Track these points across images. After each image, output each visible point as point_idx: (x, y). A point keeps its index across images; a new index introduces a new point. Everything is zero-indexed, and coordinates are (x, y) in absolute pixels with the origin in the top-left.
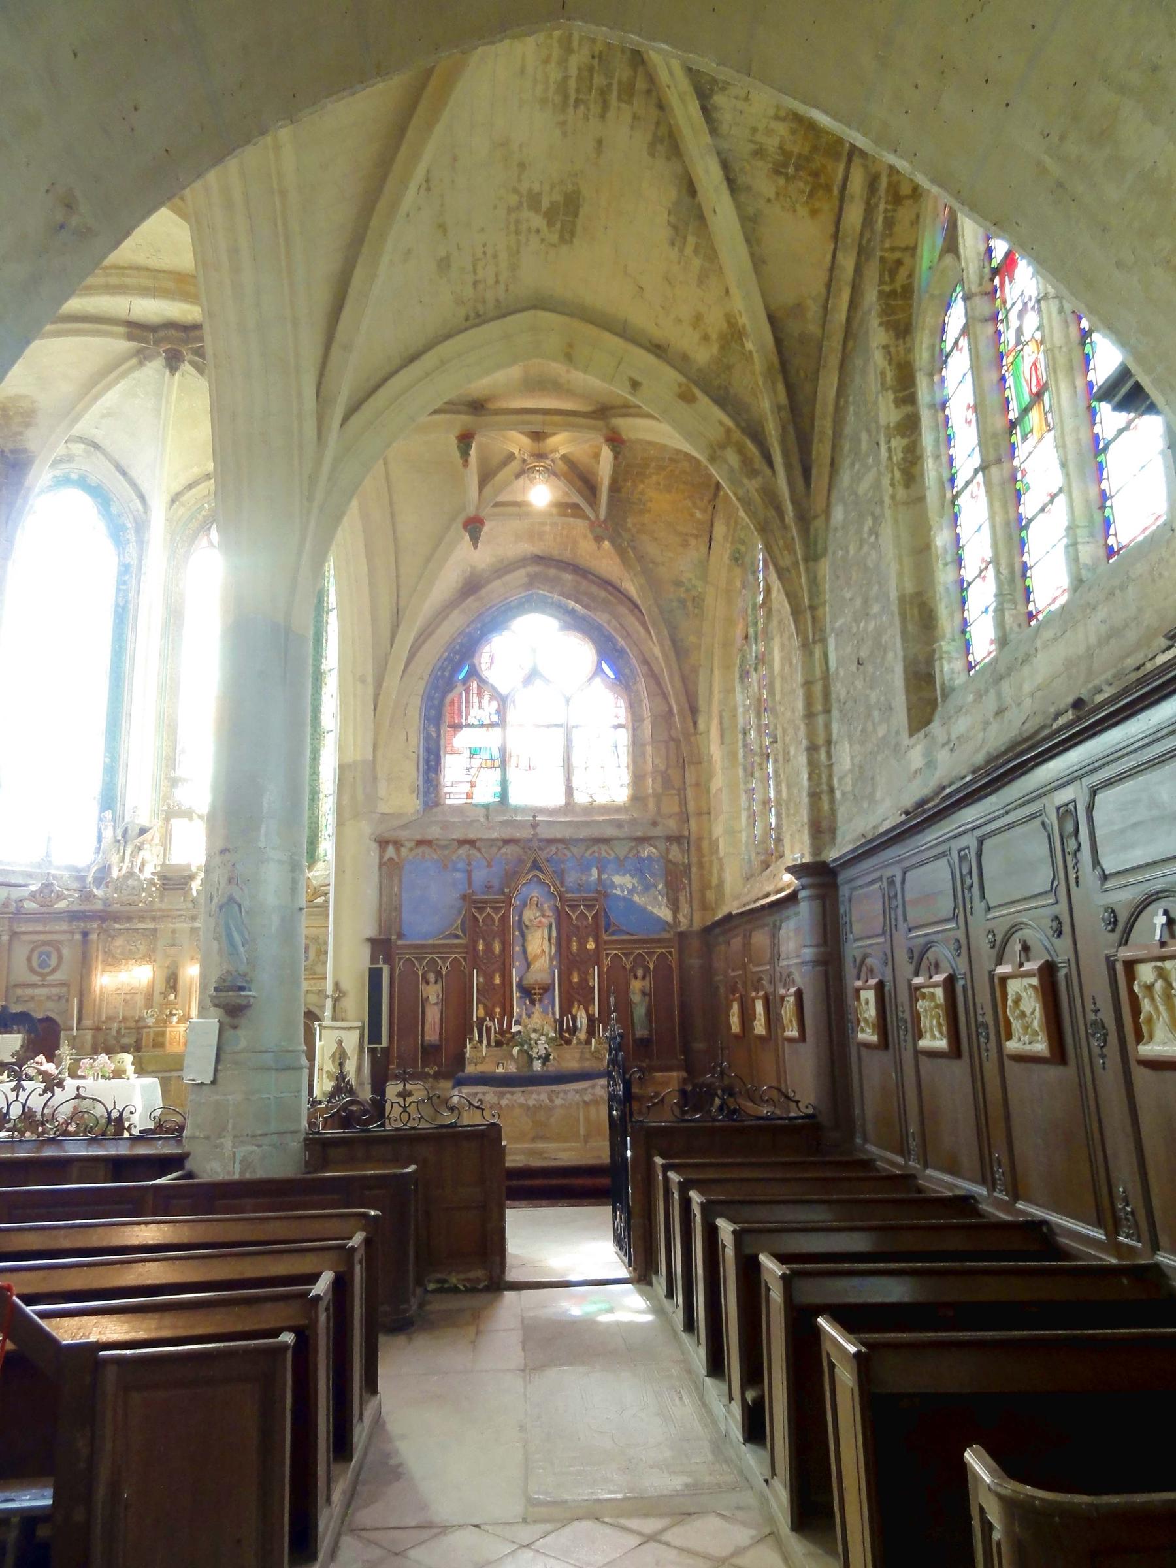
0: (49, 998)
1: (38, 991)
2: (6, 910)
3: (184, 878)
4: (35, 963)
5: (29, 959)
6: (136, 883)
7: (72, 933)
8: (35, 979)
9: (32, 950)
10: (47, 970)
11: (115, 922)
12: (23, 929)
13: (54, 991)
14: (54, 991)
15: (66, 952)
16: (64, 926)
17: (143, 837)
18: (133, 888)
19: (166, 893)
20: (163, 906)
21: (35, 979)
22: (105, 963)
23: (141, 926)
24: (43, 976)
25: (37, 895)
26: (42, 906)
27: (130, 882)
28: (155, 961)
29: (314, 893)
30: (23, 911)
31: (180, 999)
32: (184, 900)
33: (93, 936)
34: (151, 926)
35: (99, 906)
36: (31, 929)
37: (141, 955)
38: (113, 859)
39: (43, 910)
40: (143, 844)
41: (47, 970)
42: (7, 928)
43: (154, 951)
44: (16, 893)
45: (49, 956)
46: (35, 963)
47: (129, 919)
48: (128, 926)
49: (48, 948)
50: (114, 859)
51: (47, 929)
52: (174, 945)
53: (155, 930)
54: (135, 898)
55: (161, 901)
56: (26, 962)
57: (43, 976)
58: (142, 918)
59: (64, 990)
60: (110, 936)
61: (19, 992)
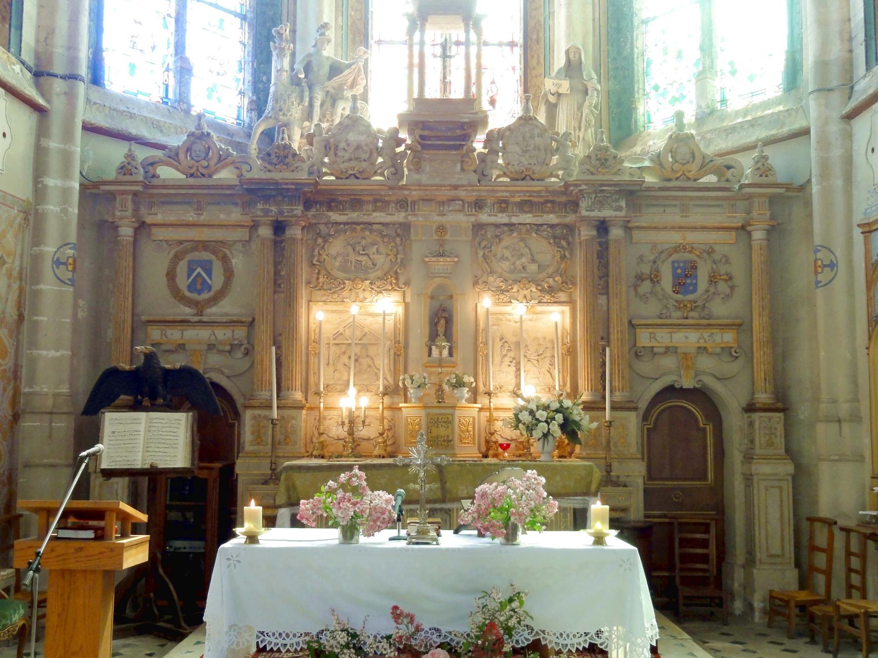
0: (211, 347)
1: (190, 334)
2: (127, 178)
3: (462, 126)
4: (182, 282)
5: (171, 276)
6: (362, 138)
7: (254, 227)
8: (186, 311)
9: (177, 258)
10: (205, 296)
11: (330, 209)
12: (159, 218)
13: (222, 334)
14: (222, 334)
15: (237, 262)
16: (235, 215)
17: (337, 80)
18: (358, 147)
19: (427, 154)
20: (424, 179)
21: (186, 311)
22: (315, 286)
23: (379, 217)
24: (199, 307)
25: (182, 156)
26: (192, 175)
27: (352, 137)
28: (407, 283)
29: (702, 166)
30: (155, 182)
31: (459, 356)
32: (463, 170)
33: (295, 232)
34: (399, 217)
35: (302, 176)
36: (172, 219)
37: (379, 273)
38: (293, 111)
39: (192, 181)
40: (340, 88)
41: (205, 296)
42: (129, 213)
43: (403, 265)
44: (142, 154)
45: (208, 268)
46: (182, 282)
47: (356, 203)
48: (354, 216)
49: (205, 255)
50: (296, 112)
51: (204, 218)
52: (442, 255)
53: (406, 227)
54: (364, 165)
55: (417, 166)
56: (164, 279)
57: (199, 307)
58: (380, 203)
59: (241, 333)
60: (319, 235)
61: (155, 333)
